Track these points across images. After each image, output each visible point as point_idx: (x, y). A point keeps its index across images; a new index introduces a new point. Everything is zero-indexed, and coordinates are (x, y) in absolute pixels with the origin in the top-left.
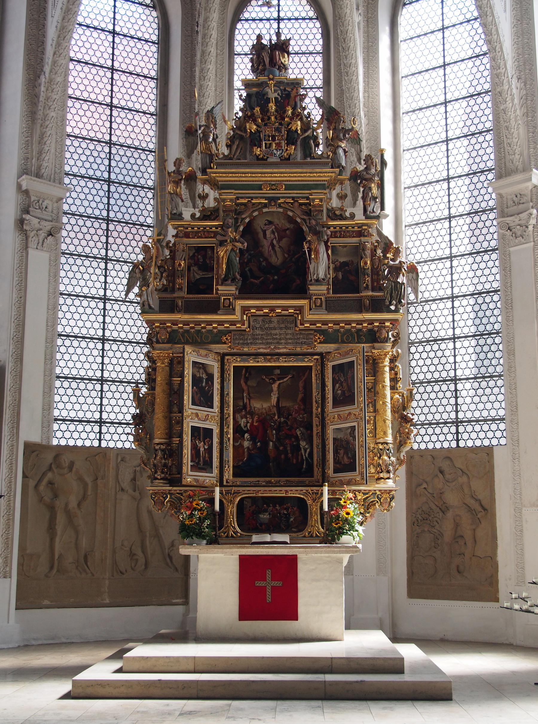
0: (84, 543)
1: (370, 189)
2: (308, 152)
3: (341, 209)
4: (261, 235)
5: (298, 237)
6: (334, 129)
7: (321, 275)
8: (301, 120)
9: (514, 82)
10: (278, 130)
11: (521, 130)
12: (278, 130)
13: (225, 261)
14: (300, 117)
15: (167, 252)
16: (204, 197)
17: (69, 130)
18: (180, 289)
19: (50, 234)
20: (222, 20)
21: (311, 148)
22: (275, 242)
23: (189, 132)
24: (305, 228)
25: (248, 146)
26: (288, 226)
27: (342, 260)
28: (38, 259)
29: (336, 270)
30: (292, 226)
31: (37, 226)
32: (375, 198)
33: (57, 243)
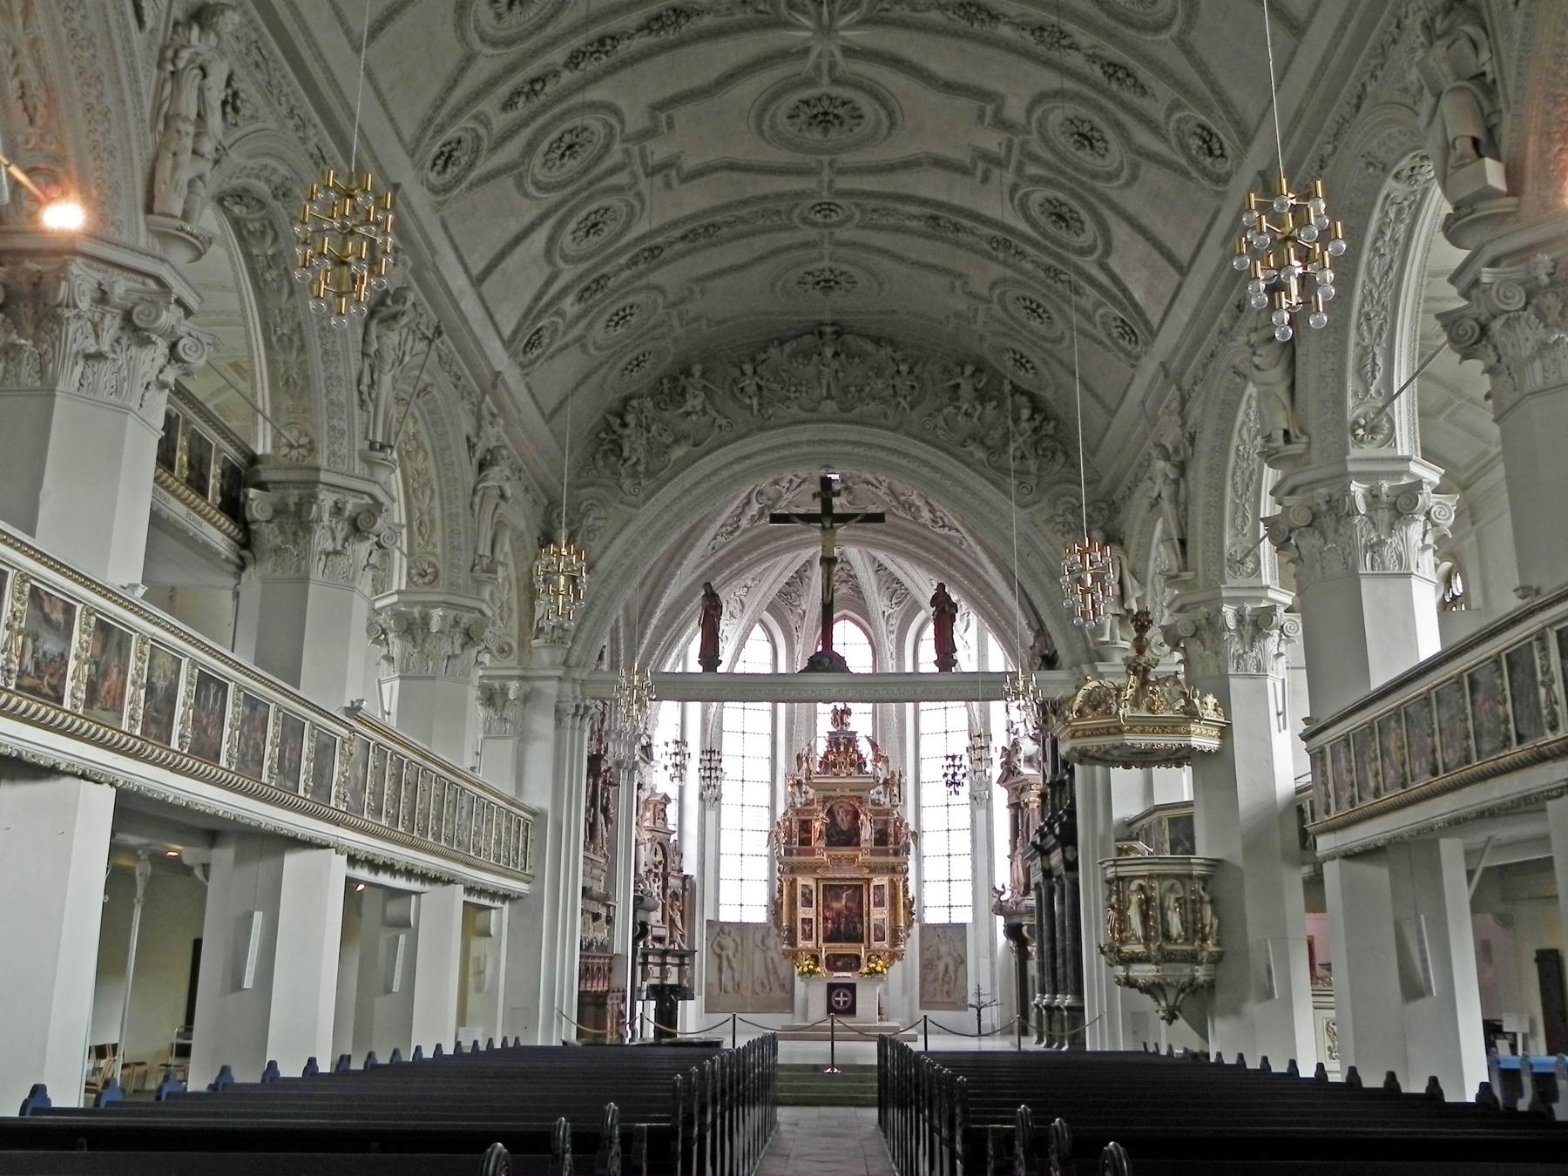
0: (737, 976)
2: (860, 770)
5: (856, 816)
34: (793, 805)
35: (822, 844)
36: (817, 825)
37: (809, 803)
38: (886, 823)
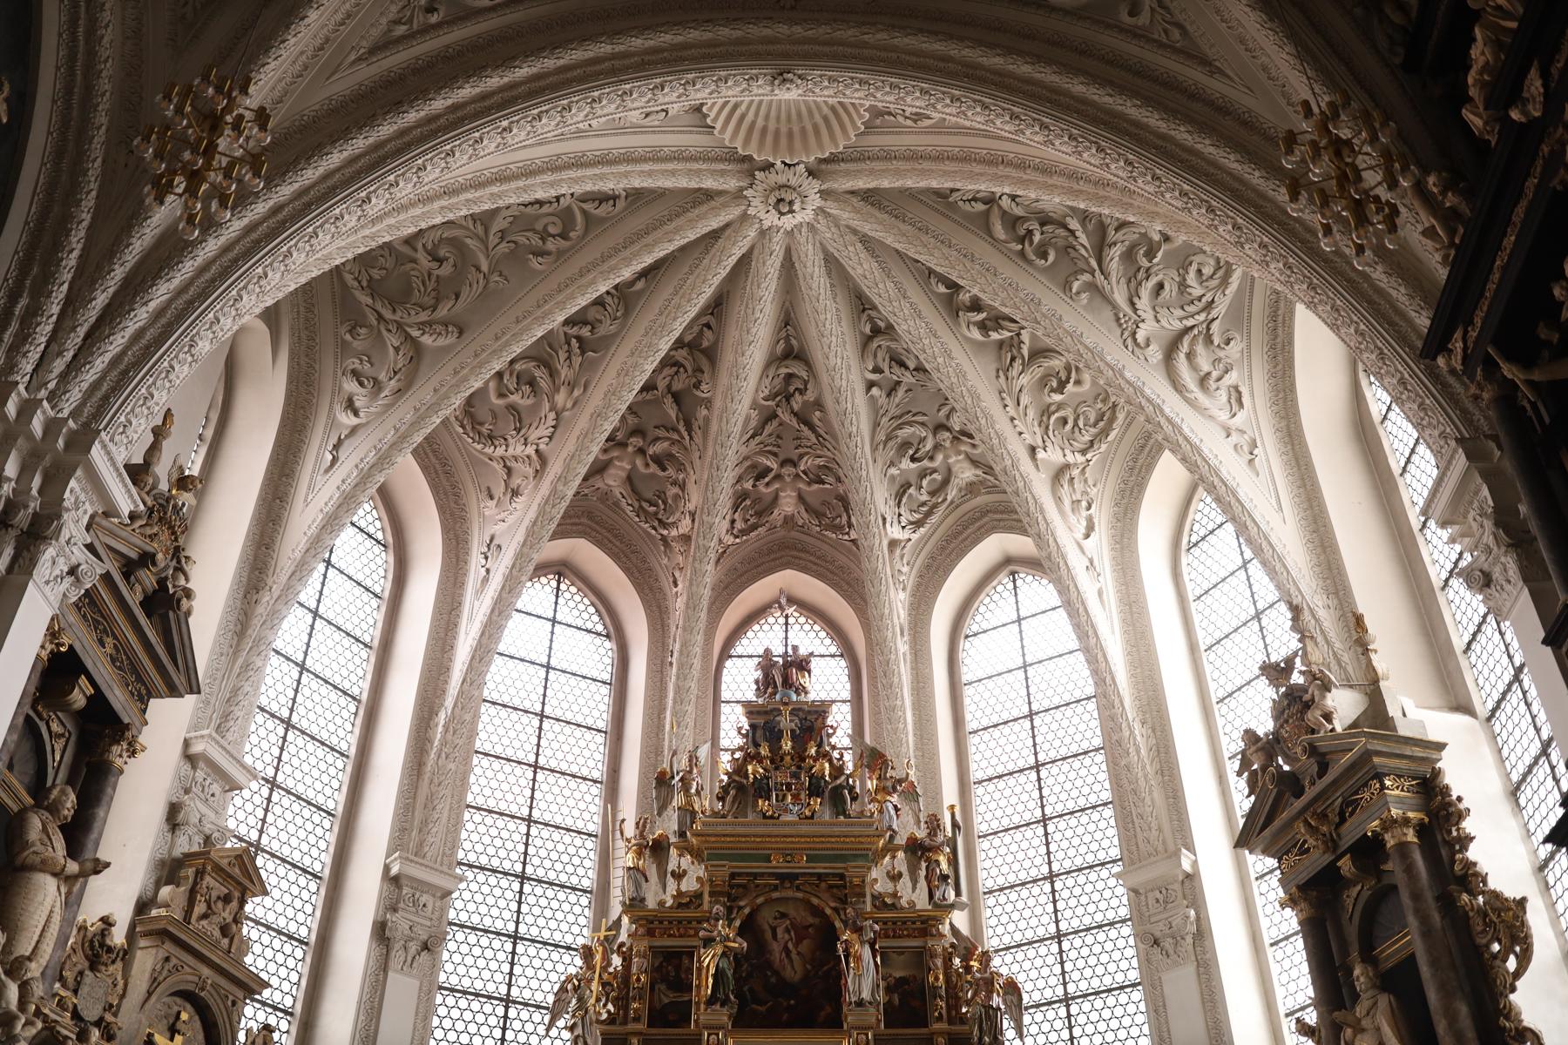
1: (938, 863)
3: (895, 895)
4: (769, 935)
5: (829, 936)
6: (879, 778)
7: (866, 995)
8: (830, 761)
9: (1137, 727)
10: (796, 776)
11: (1155, 794)
12: (796, 776)
13: (712, 971)
14: (827, 756)
15: (617, 961)
16: (678, 876)
17: (470, 799)
18: (637, 1019)
19: (425, 947)
20: (705, 668)
21: (845, 802)
22: (790, 945)
23: (663, 781)
24: (838, 924)
25: (751, 799)
26: (811, 920)
27: (898, 974)
28: (401, 988)
29: (889, 990)
30: (817, 921)
31: (407, 932)
32: (945, 878)
33: (435, 966)
34: (634, 905)
35: (723, 1015)
36: (709, 959)
37: (688, 901)
38: (921, 958)
